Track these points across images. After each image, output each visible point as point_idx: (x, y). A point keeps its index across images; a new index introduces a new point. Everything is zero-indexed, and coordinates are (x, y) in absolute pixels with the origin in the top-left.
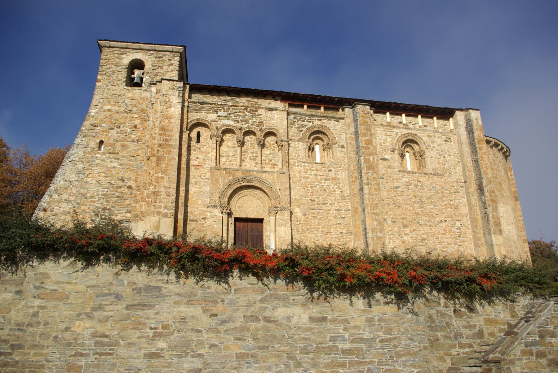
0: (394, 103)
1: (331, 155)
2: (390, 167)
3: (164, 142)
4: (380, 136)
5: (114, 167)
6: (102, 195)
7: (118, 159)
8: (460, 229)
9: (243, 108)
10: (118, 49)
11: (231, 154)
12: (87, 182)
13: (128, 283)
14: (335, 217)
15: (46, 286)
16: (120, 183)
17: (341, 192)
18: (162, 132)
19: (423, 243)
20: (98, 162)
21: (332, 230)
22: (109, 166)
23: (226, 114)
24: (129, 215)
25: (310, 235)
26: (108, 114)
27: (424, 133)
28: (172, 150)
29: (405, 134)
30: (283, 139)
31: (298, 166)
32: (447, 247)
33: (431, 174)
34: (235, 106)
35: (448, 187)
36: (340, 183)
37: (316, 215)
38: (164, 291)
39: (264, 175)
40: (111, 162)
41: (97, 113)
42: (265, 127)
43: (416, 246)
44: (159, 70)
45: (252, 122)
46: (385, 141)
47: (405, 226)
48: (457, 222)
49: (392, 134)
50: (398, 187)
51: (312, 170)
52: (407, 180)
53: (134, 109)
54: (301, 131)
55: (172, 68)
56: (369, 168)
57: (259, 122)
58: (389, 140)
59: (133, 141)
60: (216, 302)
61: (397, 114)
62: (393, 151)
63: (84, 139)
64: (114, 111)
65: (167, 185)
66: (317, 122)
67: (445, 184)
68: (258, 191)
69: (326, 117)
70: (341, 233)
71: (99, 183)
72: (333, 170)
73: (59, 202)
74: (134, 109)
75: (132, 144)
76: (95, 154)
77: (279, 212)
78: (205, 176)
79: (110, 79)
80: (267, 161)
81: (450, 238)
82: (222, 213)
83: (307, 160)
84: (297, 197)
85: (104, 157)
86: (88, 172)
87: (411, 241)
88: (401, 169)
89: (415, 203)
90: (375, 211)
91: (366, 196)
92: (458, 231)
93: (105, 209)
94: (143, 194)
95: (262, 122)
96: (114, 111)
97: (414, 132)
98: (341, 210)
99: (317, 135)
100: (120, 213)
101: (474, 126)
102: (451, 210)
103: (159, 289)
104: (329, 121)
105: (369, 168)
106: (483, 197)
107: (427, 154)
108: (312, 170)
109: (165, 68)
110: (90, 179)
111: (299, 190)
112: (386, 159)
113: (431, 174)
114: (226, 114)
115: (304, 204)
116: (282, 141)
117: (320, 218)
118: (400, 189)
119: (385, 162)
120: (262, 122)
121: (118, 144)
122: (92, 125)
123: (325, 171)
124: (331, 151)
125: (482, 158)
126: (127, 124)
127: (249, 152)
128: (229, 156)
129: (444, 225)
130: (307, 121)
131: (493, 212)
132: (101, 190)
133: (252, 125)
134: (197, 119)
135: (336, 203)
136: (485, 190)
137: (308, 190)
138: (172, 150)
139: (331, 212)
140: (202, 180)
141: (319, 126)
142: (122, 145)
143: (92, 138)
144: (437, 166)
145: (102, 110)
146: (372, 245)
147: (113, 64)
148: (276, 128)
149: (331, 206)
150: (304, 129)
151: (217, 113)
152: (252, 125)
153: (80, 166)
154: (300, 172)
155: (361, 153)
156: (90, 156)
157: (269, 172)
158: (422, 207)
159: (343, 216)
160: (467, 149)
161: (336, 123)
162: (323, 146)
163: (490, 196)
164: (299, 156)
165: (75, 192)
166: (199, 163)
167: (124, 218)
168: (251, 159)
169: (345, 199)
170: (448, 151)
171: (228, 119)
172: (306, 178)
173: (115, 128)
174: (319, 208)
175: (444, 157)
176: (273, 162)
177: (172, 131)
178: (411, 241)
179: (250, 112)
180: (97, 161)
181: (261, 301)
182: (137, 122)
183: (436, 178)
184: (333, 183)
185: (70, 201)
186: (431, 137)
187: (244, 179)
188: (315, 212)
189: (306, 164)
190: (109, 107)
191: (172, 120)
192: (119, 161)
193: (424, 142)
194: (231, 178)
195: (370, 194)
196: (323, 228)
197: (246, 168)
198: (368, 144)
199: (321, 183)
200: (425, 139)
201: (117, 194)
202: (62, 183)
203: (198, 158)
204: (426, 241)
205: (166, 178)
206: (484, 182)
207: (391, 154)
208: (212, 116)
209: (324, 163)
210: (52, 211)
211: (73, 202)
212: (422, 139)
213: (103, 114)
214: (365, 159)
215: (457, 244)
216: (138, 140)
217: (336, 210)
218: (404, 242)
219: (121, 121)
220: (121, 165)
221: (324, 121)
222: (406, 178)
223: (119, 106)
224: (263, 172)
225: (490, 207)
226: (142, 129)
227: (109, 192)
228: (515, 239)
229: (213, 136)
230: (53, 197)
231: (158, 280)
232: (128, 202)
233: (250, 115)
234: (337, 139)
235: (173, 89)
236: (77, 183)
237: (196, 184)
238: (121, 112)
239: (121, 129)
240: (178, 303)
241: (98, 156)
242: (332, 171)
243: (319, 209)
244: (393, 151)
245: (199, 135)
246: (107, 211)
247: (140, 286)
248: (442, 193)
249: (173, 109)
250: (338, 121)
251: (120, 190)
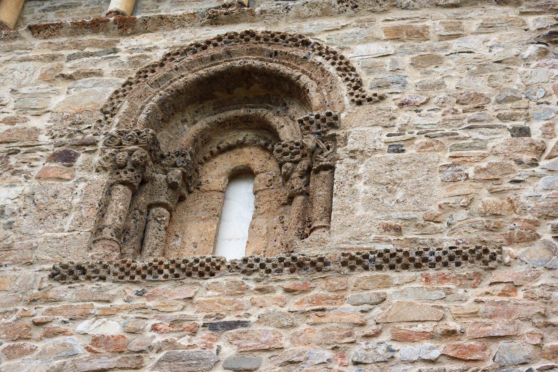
33: (355, 262)
52: (112, 328)
67: (498, 327)
113: (355, 262)
144: (441, 194)
175: (524, 132)
183: (406, 291)
186: (421, 35)
193: (346, 68)
222: (109, 314)
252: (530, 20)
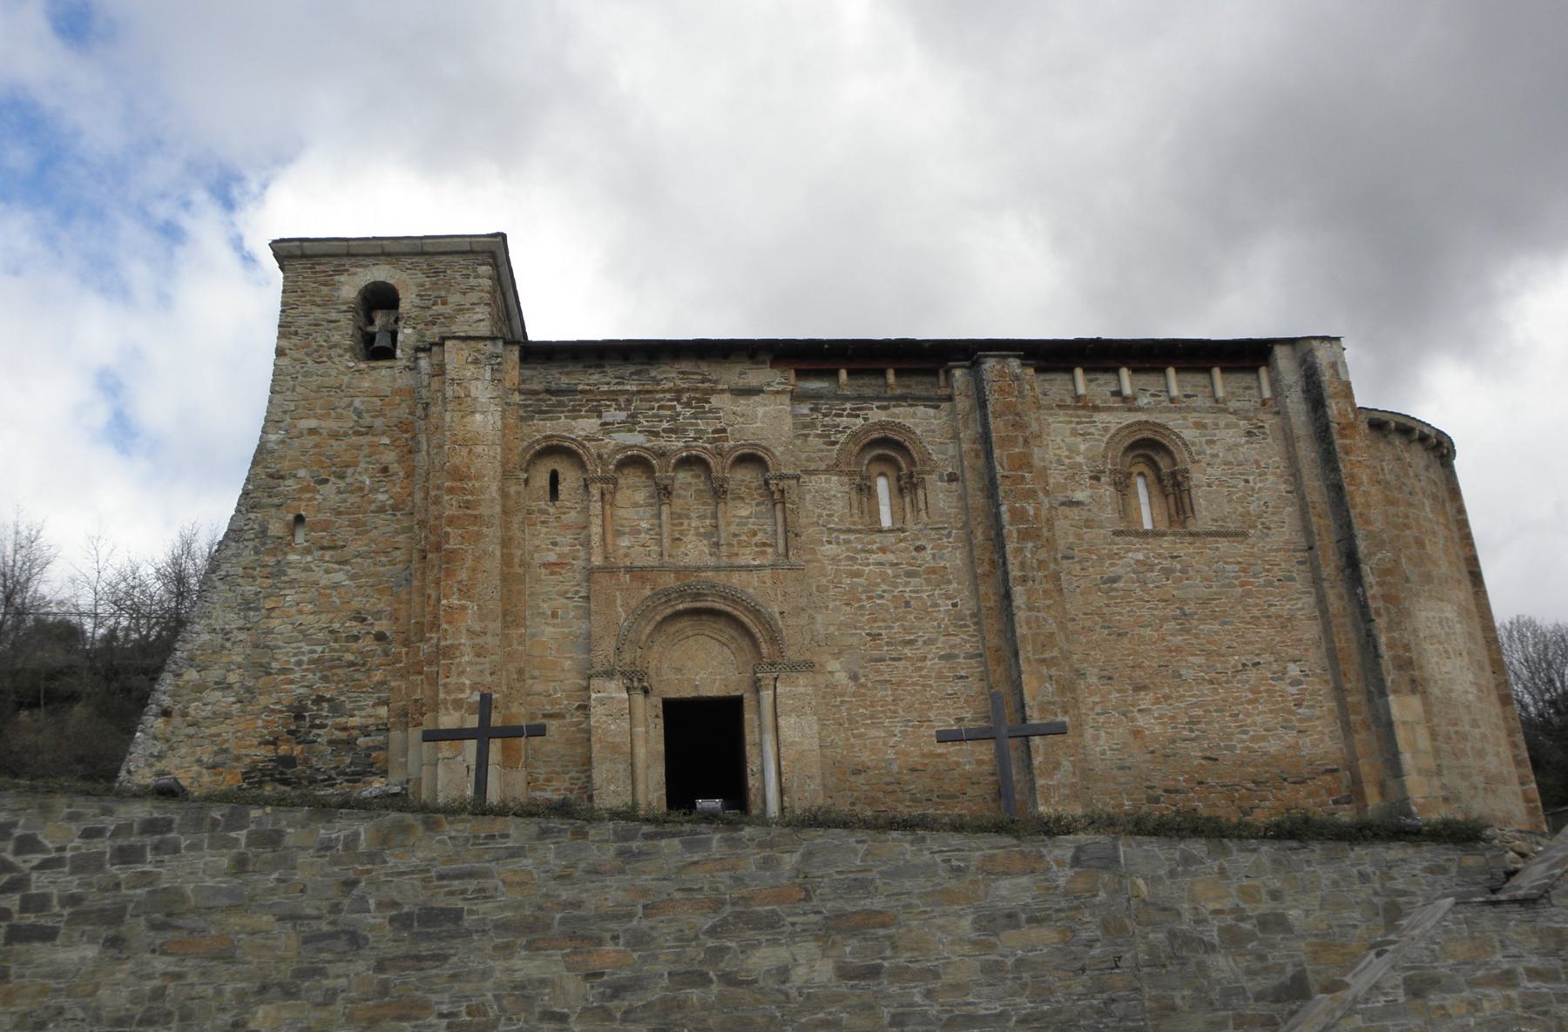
0: (1092, 340)
1: (922, 505)
2: (1088, 524)
3: (460, 512)
4: (1059, 440)
5: (336, 586)
6: (311, 662)
7: (345, 562)
8: (1301, 683)
9: (668, 396)
10: (324, 260)
11: (644, 525)
12: (269, 632)
13: (380, 905)
14: (940, 676)
15: (180, 922)
16: (355, 627)
17: (955, 605)
18: (454, 484)
19: (1191, 730)
20: (292, 573)
21: (932, 715)
22: (322, 583)
23: (622, 415)
24: (383, 711)
25: (873, 733)
26: (309, 441)
27: (1185, 418)
28: (485, 530)
29: (1128, 426)
30: (784, 471)
31: (830, 543)
32: (1263, 739)
33: (1210, 534)
34: (648, 392)
35: (1259, 568)
36: (950, 582)
38: (468, 921)
39: (736, 579)
40: (327, 572)
41: (283, 442)
42: (732, 443)
43: (1174, 742)
44: (439, 308)
45: (697, 431)
46: (1073, 450)
47: (1138, 688)
48: (1291, 666)
49: (1092, 430)
50: (1114, 580)
51: (870, 552)
52: (1140, 556)
53: (379, 422)
54: (834, 443)
55: (473, 297)
56: (1024, 536)
57: (715, 432)
58: (1082, 447)
59: (381, 510)
60: (600, 942)
61: (1106, 370)
62: (1097, 478)
63: (252, 516)
64: (324, 432)
65: (477, 628)
66: (876, 415)
67: (1252, 560)
68: (721, 624)
69: (903, 398)
71: (301, 632)
72: (929, 547)
73: (200, 688)
74: (379, 422)
75: (380, 520)
76: (286, 554)
77: (783, 676)
78: (577, 592)
79: (309, 346)
80: (744, 538)
81: (1271, 711)
82: (628, 690)
83: (854, 523)
84: (832, 629)
85: (309, 558)
86: (269, 604)
87: (1157, 729)
88: (1122, 527)
89: (1165, 619)
90: (1047, 655)
91: (1021, 615)
92: (1294, 690)
93: (320, 700)
94: (416, 655)
95: (724, 431)
96: (324, 432)
97: (1152, 418)
98: (956, 656)
99: (886, 452)
100: (361, 708)
101: (1325, 386)
102: (1272, 632)
103: (456, 915)
104: (912, 410)
105: (1024, 536)
106: (1360, 591)
107: (1197, 477)
109: (455, 298)
110: (278, 621)
111: (836, 609)
112: (1078, 503)
113: (1210, 534)
114: (622, 415)
115: (850, 647)
116: (782, 477)
117: (898, 684)
118: (1121, 585)
119: (1076, 510)
120: (724, 431)
121: (344, 520)
122: (271, 476)
123: (907, 549)
124: (920, 492)
125: (1352, 476)
126: (363, 465)
127: (694, 515)
128: (639, 532)
129: (1253, 674)
130: (849, 415)
131: (1389, 629)
132: (306, 648)
133: (695, 439)
134: (547, 438)
135: (942, 639)
136: (1365, 569)
137: (862, 607)
138: (485, 530)
140: (571, 604)
141: (882, 426)
142: (355, 524)
143: (273, 511)
144: (1227, 509)
145: (295, 432)
146: (1041, 750)
147: (314, 303)
148: (764, 443)
149: (927, 648)
150: (842, 438)
151: (600, 416)
152: (695, 439)
153: (249, 589)
154: (835, 559)
155: (1001, 494)
156: (271, 561)
157: (748, 568)
158: (1187, 631)
159: (963, 673)
160: (1307, 452)
161: (931, 411)
162: (899, 479)
163: (1381, 584)
164: (830, 516)
165: (239, 659)
166: (559, 556)
167: (371, 721)
168: (698, 534)
169: (965, 626)
170: (1257, 462)
171: (630, 431)
172: (858, 574)
173: (332, 479)
174: (895, 655)
175: (1247, 481)
176: (759, 538)
177: (479, 477)
178: (1157, 729)
179: (688, 405)
180: (290, 571)
181: (713, 932)
182: (390, 457)
183: (1223, 544)
184: (928, 581)
185: (230, 686)
186: (1204, 426)
187: (682, 594)
188: (882, 666)
189: (852, 537)
190: (313, 423)
191: (479, 449)
192: (348, 567)
193: (1185, 444)
194: (647, 592)
195: (1030, 609)
196: (910, 707)
197: (687, 559)
198: (1020, 468)
199: (895, 585)
200: (1189, 434)
201: (349, 657)
202: (206, 637)
203: (555, 544)
204: (1203, 726)
205: (472, 607)
206: (1362, 546)
207: (1091, 487)
208: (586, 426)
209: (902, 530)
210: (184, 714)
211: (236, 686)
212: (1178, 436)
213: (297, 442)
214: (1012, 511)
215: (1292, 728)
216: (395, 508)
217: (941, 658)
218: (1137, 733)
219: (347, 457)
220: (353, 577)
221: (896, 410)
222: (1138, 550)
223: (339, 417)
224: (733, 568)
225: (1379, 615)
226: (402, 474)
227: (327, 655)
228: (1470, 697)
229: (593, 480)
230: (186, 677)
231: (452, 893)
232: (378, 676)
233: (689, 412)
234: (934, 457)
235: (476, 362)
236: (242, 636)
237: (554, 615)
238: (346, 434)
239: (348, 480)
240: (506, 950)
241: (293, 557)
242: (924, 548)
244: (1097, 478)
245: (554, 479)
246: (325, 705)
247: (406, 909)
248: (1243, 584)
249: (478, 417)
250: (937, 407)
251: (354, 646)
252: (1241, 423)
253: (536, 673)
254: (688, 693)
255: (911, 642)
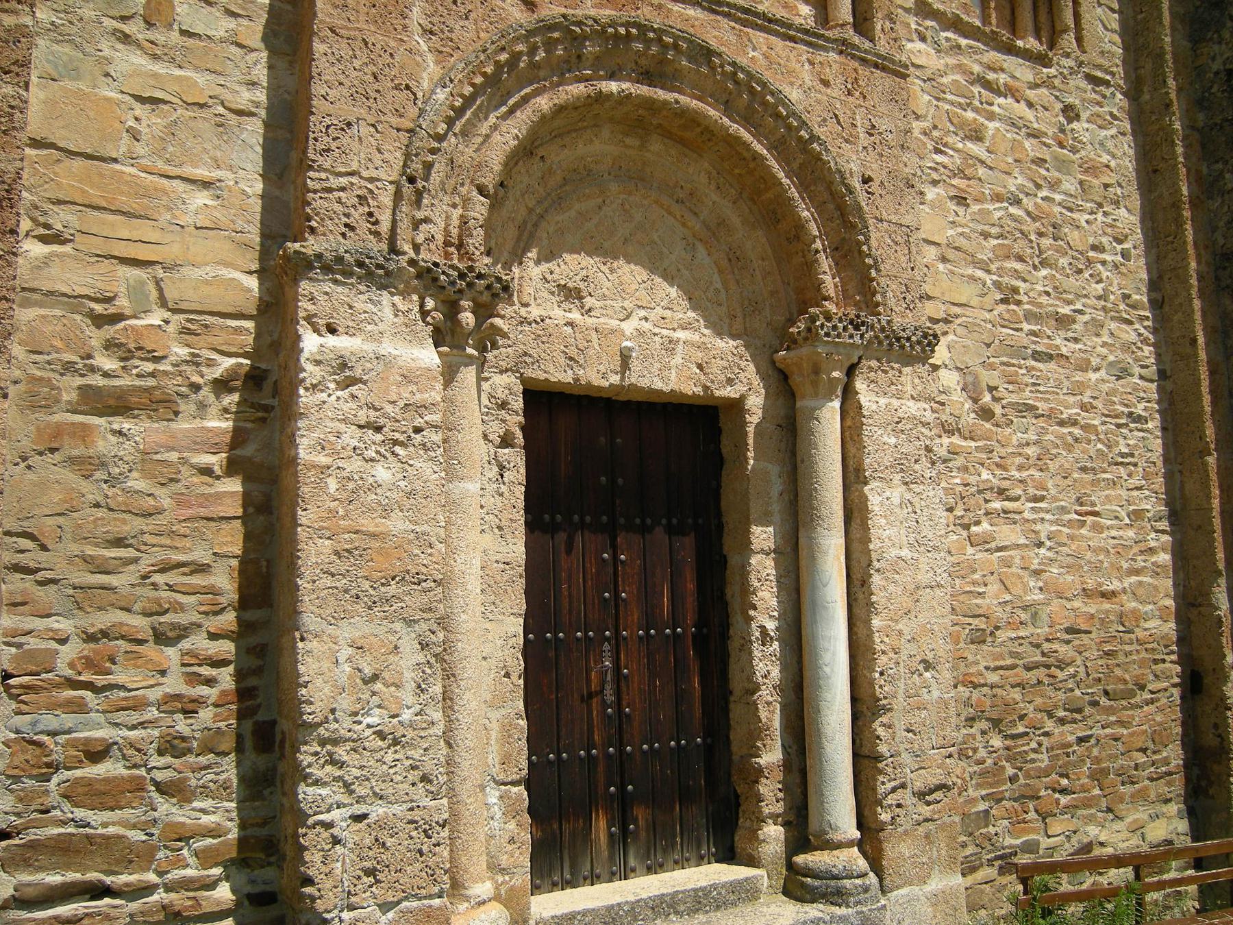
25: (1008, 534)
37: (1027, 396)
70: (1137, 515)
72: (1084, 116)
108: (987, 85)
139: (1094, 376)
243: (1037, 356)
253: (61, 218)
254: (599, 374)
255: (1063, 322)
